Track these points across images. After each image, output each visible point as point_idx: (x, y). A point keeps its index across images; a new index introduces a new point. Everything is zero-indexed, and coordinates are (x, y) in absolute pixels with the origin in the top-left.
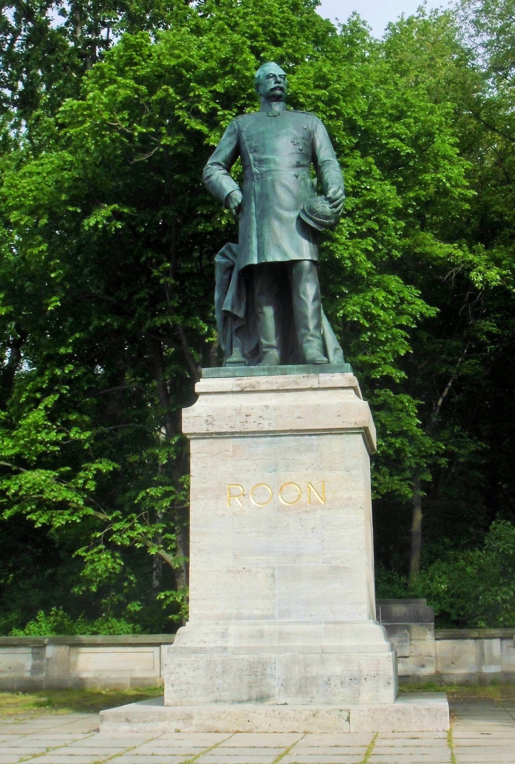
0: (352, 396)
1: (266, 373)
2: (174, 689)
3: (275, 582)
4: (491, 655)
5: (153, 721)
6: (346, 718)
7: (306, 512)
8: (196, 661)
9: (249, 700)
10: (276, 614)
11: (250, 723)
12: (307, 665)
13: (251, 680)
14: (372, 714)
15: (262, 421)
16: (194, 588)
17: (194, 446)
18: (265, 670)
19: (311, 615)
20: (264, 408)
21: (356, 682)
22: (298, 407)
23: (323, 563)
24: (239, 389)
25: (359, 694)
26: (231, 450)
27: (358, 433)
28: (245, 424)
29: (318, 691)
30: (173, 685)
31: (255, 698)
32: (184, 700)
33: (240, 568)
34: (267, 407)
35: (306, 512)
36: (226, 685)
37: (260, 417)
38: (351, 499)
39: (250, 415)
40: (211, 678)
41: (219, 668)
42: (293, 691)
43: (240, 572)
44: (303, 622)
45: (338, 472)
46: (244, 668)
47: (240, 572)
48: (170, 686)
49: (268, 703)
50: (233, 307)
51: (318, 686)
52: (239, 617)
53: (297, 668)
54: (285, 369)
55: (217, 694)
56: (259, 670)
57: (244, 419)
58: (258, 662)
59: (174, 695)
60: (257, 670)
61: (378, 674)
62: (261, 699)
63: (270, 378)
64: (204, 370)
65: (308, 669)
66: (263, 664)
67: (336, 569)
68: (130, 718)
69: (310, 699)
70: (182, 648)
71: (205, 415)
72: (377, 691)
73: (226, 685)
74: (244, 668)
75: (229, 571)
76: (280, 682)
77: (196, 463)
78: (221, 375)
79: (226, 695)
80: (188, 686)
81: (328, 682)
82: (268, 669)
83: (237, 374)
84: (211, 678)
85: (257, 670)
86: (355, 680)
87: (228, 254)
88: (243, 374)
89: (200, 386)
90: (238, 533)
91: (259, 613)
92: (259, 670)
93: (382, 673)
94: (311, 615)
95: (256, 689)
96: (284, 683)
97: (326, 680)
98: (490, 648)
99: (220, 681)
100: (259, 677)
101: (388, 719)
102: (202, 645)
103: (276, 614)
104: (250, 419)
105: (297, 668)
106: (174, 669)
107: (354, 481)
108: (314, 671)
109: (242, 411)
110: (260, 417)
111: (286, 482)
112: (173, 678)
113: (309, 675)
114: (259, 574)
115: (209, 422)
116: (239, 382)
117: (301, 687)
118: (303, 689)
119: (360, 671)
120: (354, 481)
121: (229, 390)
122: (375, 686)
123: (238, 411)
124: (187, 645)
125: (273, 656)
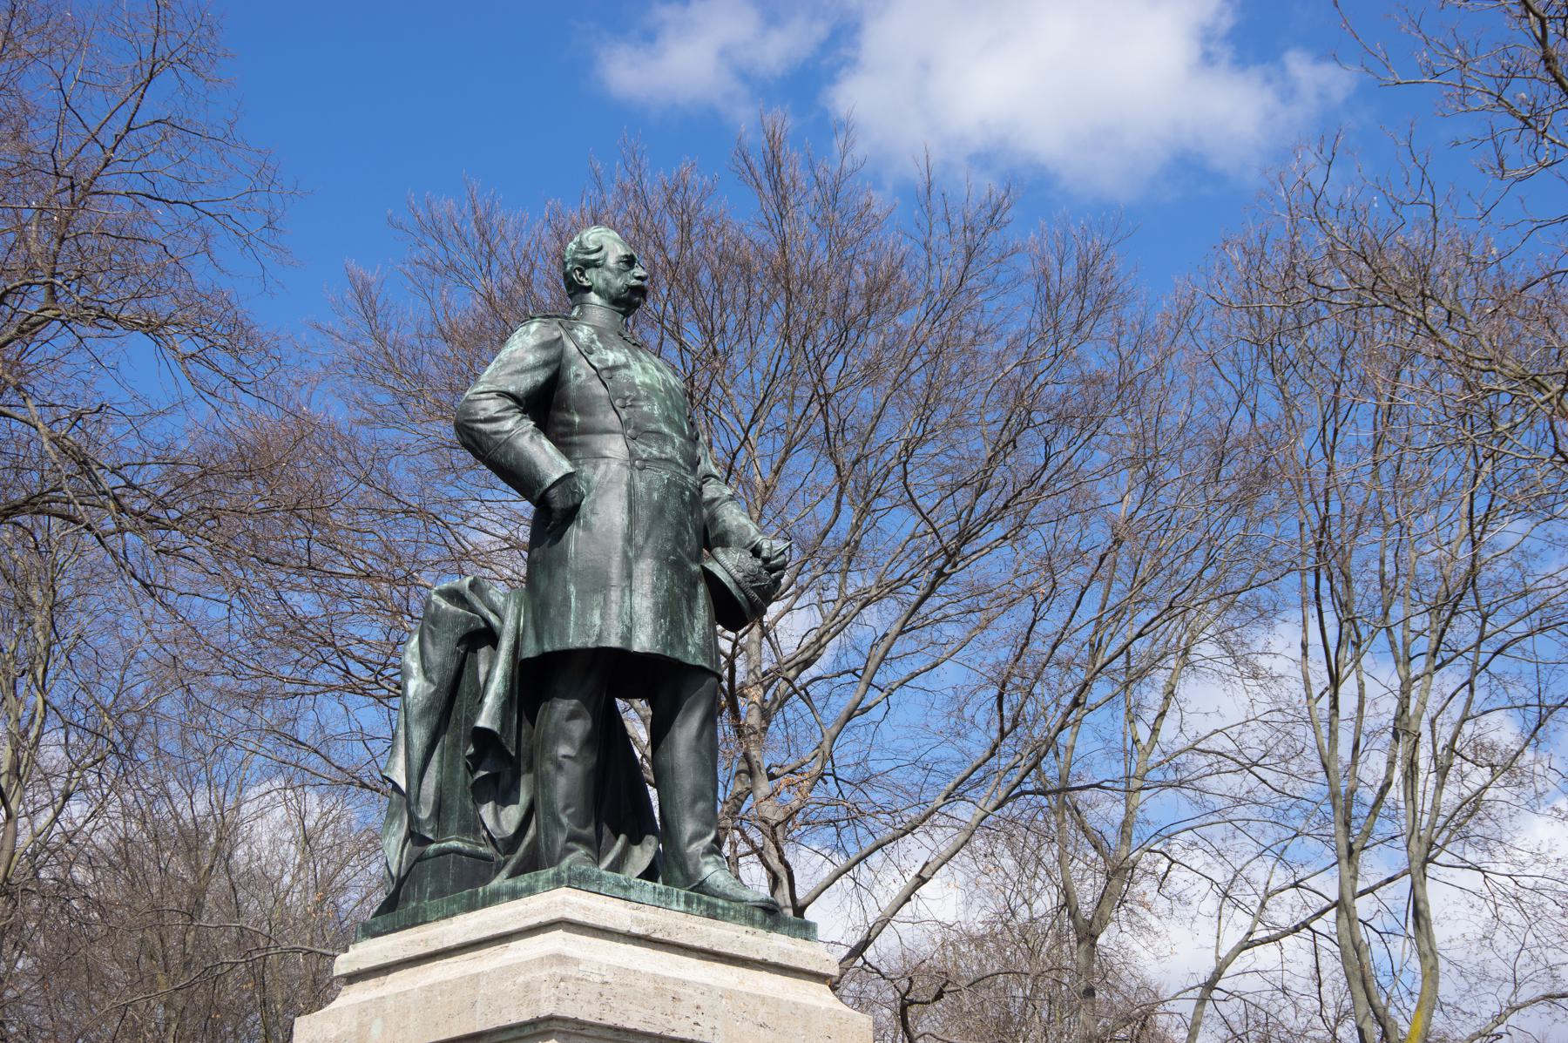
22: (763, 1000)
34: (711, 989)
71: (598, 979)
121: (623, 928)
123: (660, 983)
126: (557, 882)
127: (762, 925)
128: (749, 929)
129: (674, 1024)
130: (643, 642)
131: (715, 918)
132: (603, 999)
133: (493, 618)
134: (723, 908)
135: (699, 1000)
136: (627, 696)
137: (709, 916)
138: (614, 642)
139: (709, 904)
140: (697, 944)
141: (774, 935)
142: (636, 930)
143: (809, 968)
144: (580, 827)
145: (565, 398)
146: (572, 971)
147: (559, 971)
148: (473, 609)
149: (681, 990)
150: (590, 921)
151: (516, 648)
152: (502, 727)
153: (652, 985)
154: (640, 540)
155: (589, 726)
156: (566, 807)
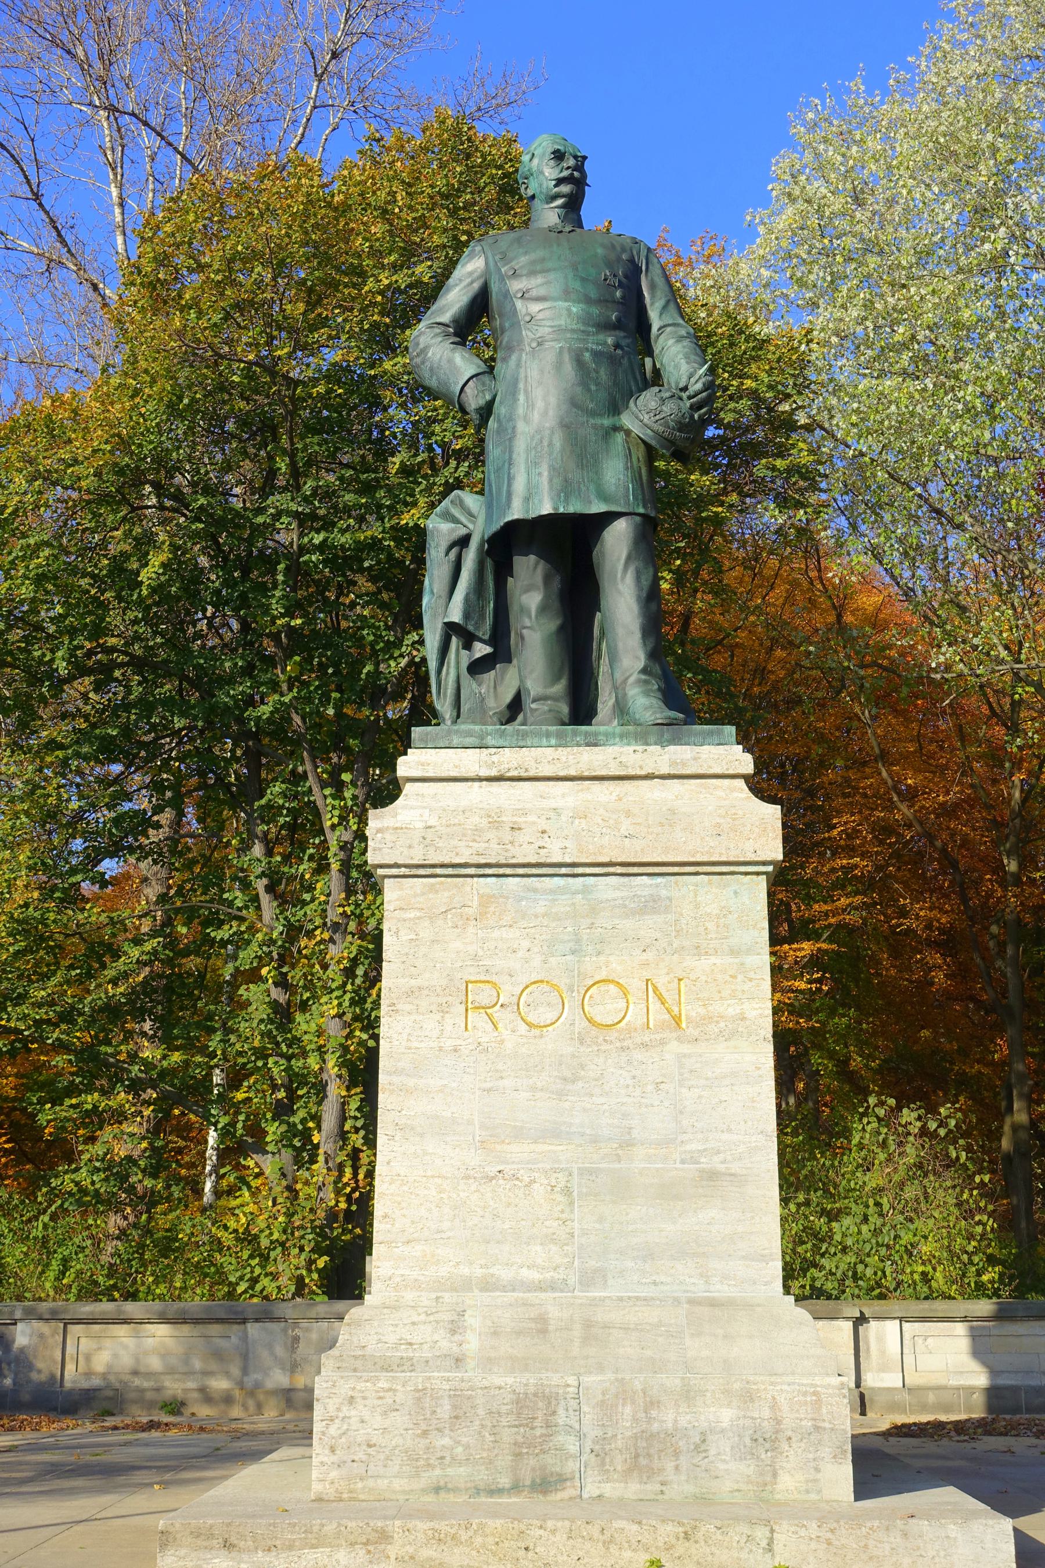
0: (744, 795)
1: (553, 742)
2: (334, 1458)
3: (571, 1203)
4: (883, 1352)
5: (290, 1548)
6: (764, 1543)
7: (644, 1045)
8: (390, 1390)
9: (516, 1488)
10: (573, 1280)
11: (530, 1554)
12: (653, 1404)
13: (520, 1439)
14: (829, 1535)
15: (546, 841)
16: (385, 1216)
17: (394, 894)
18: (554, 1413)
19: (655, 1283)
20: (552, 814)
21: (767, 1445)
23: (683, 1162)
24: (494, 773)
25: (775, 1475)
26: (475, 903)
27: (758, 874)
28: (509, 846)
29: (677, 1468)
30: (333, 1450)
31: (528, 1483)
32: (360, 1485)
33: (492, 1171)
35: (644, 1045)
36: (460, 1449)
38: (743, 1019)
40: (425, 1433)
41: (445, 1410)
42: (619, 1468)
43: (493, 1178)
44: (637, 1298)
45: (713, 959)
46: (504, 1409)
47: (493, 1178)
48: (327, 1452)
49: (560, 1495)
50: (467, 615)
51: (677, 1454)
52: (488, 1285)
53: (628, 1410)
54: (596, 734)
55: (438, 1472)
56: (539, 1414)
57: (507, 836)
58: (535, 1395)
59: (334, 1474)
60: (534, 1413)
61: (817, 1428)
62: (545, 1484)
63: (562, 753)
64: (416, 732)
65: (654, 1413)
66: (550, 1400)
67: (712, 1176)
68: (233, 1540)
69: (658, 1487)
70: (356, 1357)
71: (420, 825)
72: (817, 1470)
73: (460, 1449)
74: (504, 1409)
75: (467, 1177)
76: (588, 1445)
77: (397, 933)
78: (456, 741)
79: (459, 1473)
80: (370, 1451)
81: (700, 1447)
82: (561, 1412)
83: (490, 740)
84: (425, 1433)
85: (534, 1413)
86: (765, 1442)
87: (456, 512)
88: (501, 743)
89: (406, 765)
90: (489, 1090)
91: (535, 1276)
92: (539, 1414)
93: (827, 1425)
94: (655, 1283)
95: (532, 1462)
96: (597, 1447)
97: (697, 1439)
98: (881, 1339)
99: (446, 1441)
100: (538, 1432)
101: (866, 1546)
102: (403, 1352)
103: (573, 1280)
104: (522, 837)
105: (628, 1410)
106: (339, 1409)
107: (751, 980)
108: (668, 1417)
109: (504, 819)
111: (597, 978)
112: (333, 1431)
113: (655, 1426)
114: (536, 1186)
115: (428, 841)
116: (495, 758)
117: (637, 1456)
118: (643, 1461)
119: (779, 1422)
120: (751, 980)
121: (471, 774)
122: (811, 1456)
124: (368, 1351)
125: (572, 1380)
127: (661, 743)
128: (640, 748)
129: (514, 850)
131: (596, 745)
132: (428, 841)
134: (606, 735)
135: (543, 824)
137: (588, 745)
140: (562, 774)
141: (672, 748)
142: (484, 773)
143: (711, 771)
150: (430, 774)
153: (484, 822)
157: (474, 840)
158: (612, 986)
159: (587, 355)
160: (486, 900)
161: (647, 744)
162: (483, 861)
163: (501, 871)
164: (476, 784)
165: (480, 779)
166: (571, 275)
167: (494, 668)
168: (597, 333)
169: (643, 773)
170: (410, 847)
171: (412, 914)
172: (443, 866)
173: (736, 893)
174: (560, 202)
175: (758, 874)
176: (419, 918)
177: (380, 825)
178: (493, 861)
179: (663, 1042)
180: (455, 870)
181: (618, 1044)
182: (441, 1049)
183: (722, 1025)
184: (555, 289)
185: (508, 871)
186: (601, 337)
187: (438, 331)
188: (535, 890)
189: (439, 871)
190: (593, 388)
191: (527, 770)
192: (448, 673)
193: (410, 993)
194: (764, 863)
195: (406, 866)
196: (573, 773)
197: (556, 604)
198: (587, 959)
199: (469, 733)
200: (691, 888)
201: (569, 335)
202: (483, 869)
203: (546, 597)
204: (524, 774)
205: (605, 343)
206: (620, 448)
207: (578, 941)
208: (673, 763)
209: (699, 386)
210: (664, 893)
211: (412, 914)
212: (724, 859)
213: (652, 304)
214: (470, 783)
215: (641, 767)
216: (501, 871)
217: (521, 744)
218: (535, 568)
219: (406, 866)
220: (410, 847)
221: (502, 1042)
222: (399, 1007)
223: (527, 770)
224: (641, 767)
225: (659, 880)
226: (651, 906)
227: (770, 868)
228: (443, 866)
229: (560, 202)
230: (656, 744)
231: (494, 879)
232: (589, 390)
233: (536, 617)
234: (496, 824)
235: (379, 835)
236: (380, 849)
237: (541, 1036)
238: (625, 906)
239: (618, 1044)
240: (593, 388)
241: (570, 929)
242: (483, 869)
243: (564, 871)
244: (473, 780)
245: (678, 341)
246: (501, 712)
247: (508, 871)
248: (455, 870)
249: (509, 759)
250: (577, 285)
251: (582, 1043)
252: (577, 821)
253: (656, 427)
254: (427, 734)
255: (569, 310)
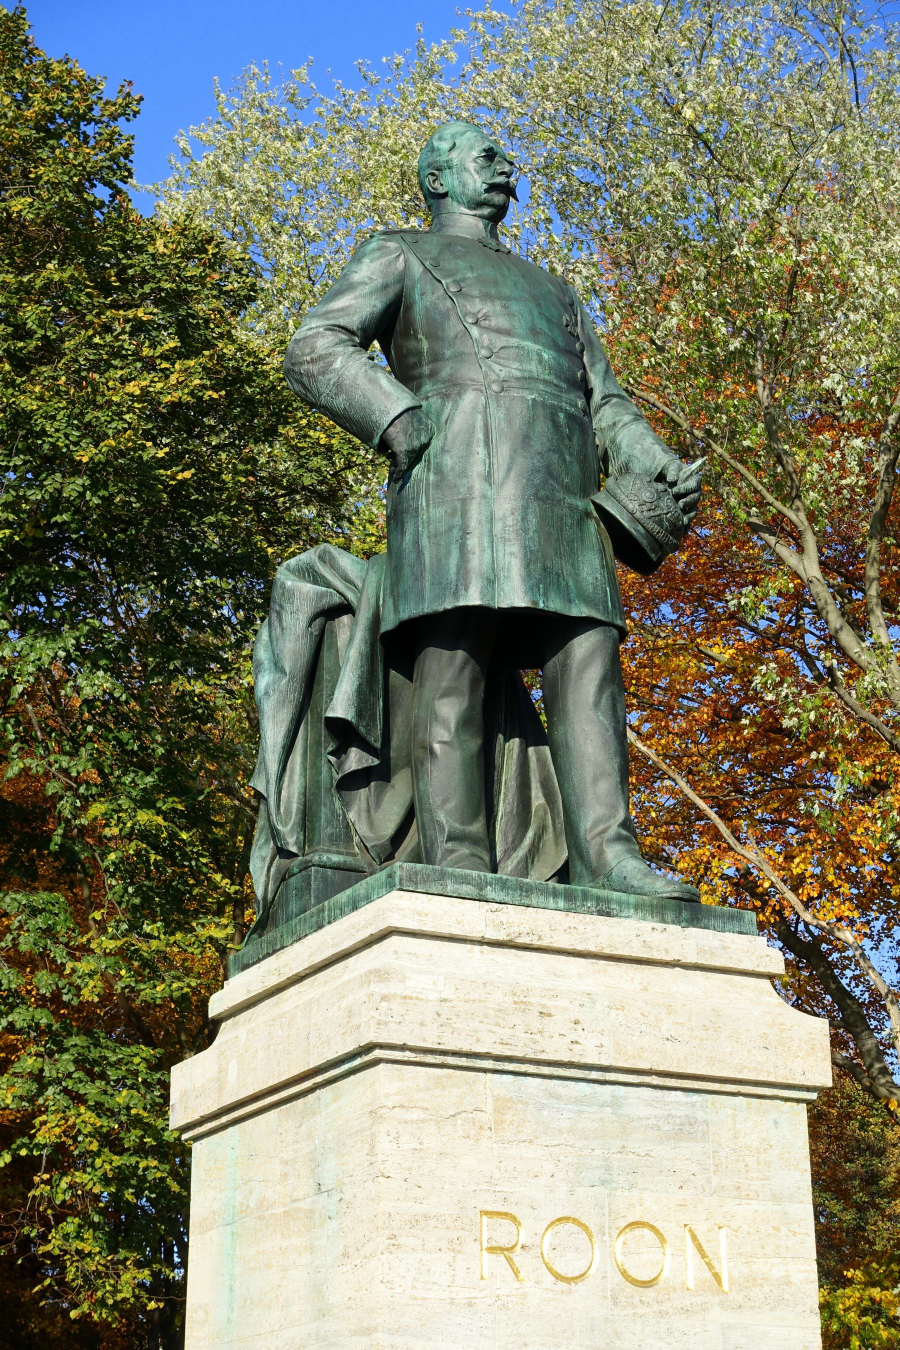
1: (561, 904)
15: (578, 1035)
24: (502, 936)
26: (490, 1108)
27: (798, 1101)
28: (538, 1037)
37: (576, 1022)
38: (789, 1283)
39: (550, 1015)
54: (608, 901)
57: (536, 1023)
63: (573, 919)
83: (489, 892)
88: (501, 896)
107: (794, 1234)
109: (531, 999)
110: (576, 1022)
115: (443, 1019)
126: (390, 886)
128: (660, 926)
130: (514, 595)
131: (608, 914)
132: (443, 1019)
133: (350, 596)
134: (620, 903)
136: (524, 669)
137: (600, 913)
138: (473, 598)
139: (598, 899)
140: (580, 947)
141: (692, 931)
144: (463, 823)
145: (409, 325)
146: (394, 988)
147: (379, 989)
148: (328, 585)
149: (551, 1003)
150: (428, 928)
151: (376, 620)
152: (359, 714)
154: (498, 476)
155: (465, 704)
156: (445, 801)
157: (498, 1024)
158: (646, 1231)
159: (562, 415)
160: (502, 1105)
161: (664, 921)
162: (508, 1053)
163: (523, 1068)
164: (477, 948)
165: (482, 942)
166: (536, 312)
167: (367, 785)
168: (568, 392)
169: (668, 958)
170: (422, 1024)
171: (415, 1115)
172: (455, 1054)
173: (776, 1122)
174: (486, 211)
175: (798, 1101)
176: (423, 1121)
177: (385, 991)
178: (520, 1054)
179: (704, 1308)
180: (469, 1061)
181: (656, 1307)
182: (452, 1301)
183: (767, 1289)
184: (520, 325)
185: (531, 1069)
186: (572, 396)
187: (345, 337)
188: (558, 1097)
189: (450, 1060)
190: (568, 458)
191: (540, 938)
192: (291, 781)
193: (414, 1222)
194: (808, 1089)
195: (413, 1049)
196: (592, 948)
197: (478, 718)
198: (619, 1193)
199: (465, 880)
200: (730, 1112)
201: (541, 387)
202: (505, 1064)
203: (471, 706)
204: (536, 943)
205: (576, 406)
206: (594, 540)
207: (608, 1168)
208: (700, 951)
209: (692, 483)
210: (700, 1115)
211: (415, 1115)
212: (771, 1079)
213: (592, 365)
214: (469, 946)
215: (667, 951)
216: (523, 1068)
217: (527, 902)
218: (462, 669)
219: (413, 1049)
220: (422, 1024)
221: (524, 1296)
222: (401, 1240)
223: (540, 938)
224: (667, 951)
225: (695, 1097)
226: (687, 1130)
227: (814, 1096)
228: (455, 1054)
229: (486, 211)
230: (673, 923)
231: (510, 1077)
232: (564, 460)
233: (457, 730)
234: (522, 1005)
235: (384, 1004)
236: (386, 1023)
237: (570, 1292)
238: (659, 1129)
239: (656, 1307)
240: (568, 458)
241: (598, 1152)
242: (505, 1064)
243: (594, 1075)
244: (472, 941)
245: (635, 420)
246: (383, 846)
247: (531, 1069)
248: (469, 1061)
249: (516, 920)
250: (542, 325)
251: (615, 1304)
252: (613, 1013)
253: (651, 525)
254: (416, 873)
255: (539, 355)
